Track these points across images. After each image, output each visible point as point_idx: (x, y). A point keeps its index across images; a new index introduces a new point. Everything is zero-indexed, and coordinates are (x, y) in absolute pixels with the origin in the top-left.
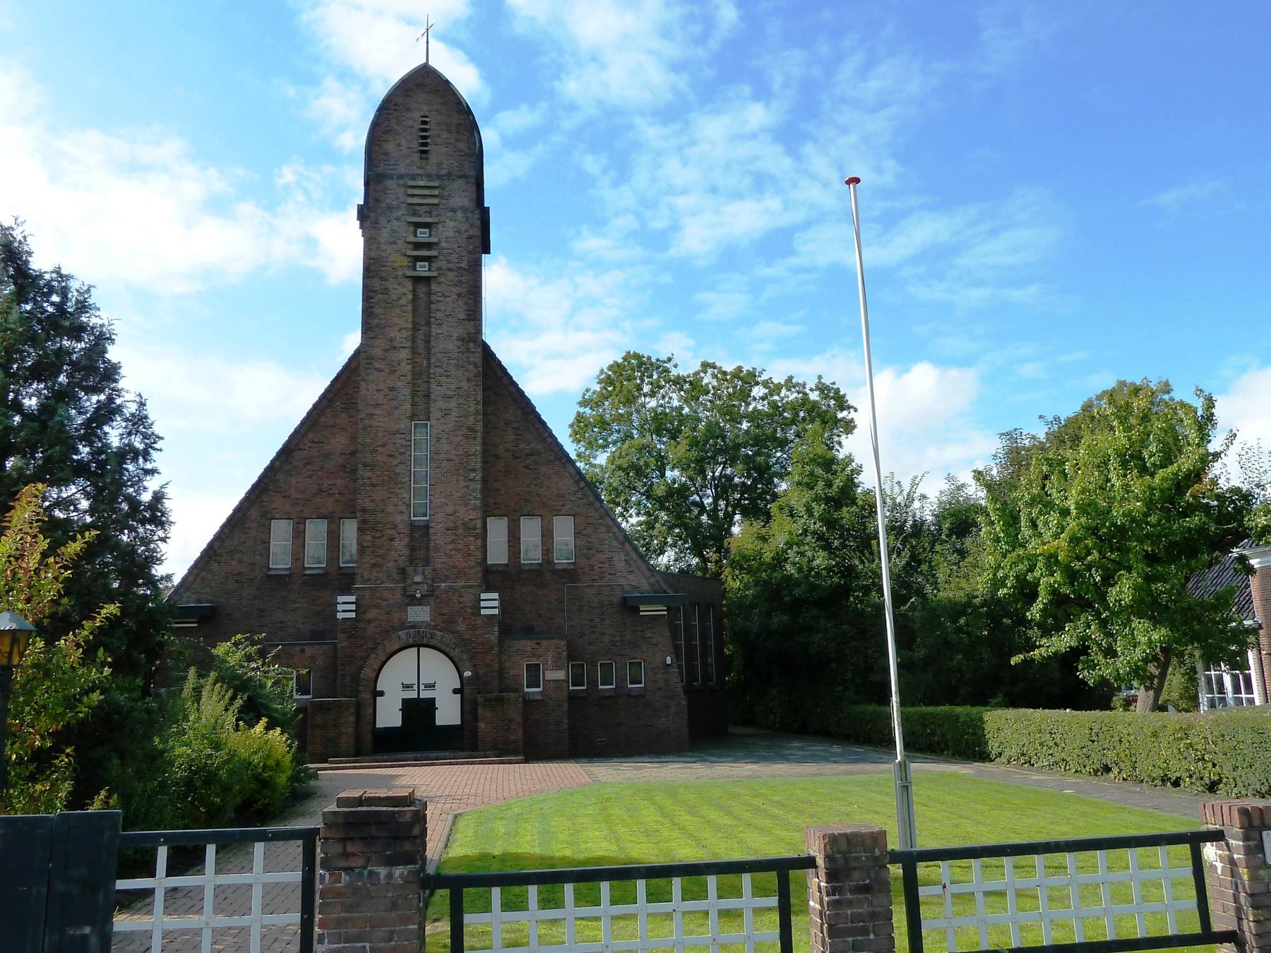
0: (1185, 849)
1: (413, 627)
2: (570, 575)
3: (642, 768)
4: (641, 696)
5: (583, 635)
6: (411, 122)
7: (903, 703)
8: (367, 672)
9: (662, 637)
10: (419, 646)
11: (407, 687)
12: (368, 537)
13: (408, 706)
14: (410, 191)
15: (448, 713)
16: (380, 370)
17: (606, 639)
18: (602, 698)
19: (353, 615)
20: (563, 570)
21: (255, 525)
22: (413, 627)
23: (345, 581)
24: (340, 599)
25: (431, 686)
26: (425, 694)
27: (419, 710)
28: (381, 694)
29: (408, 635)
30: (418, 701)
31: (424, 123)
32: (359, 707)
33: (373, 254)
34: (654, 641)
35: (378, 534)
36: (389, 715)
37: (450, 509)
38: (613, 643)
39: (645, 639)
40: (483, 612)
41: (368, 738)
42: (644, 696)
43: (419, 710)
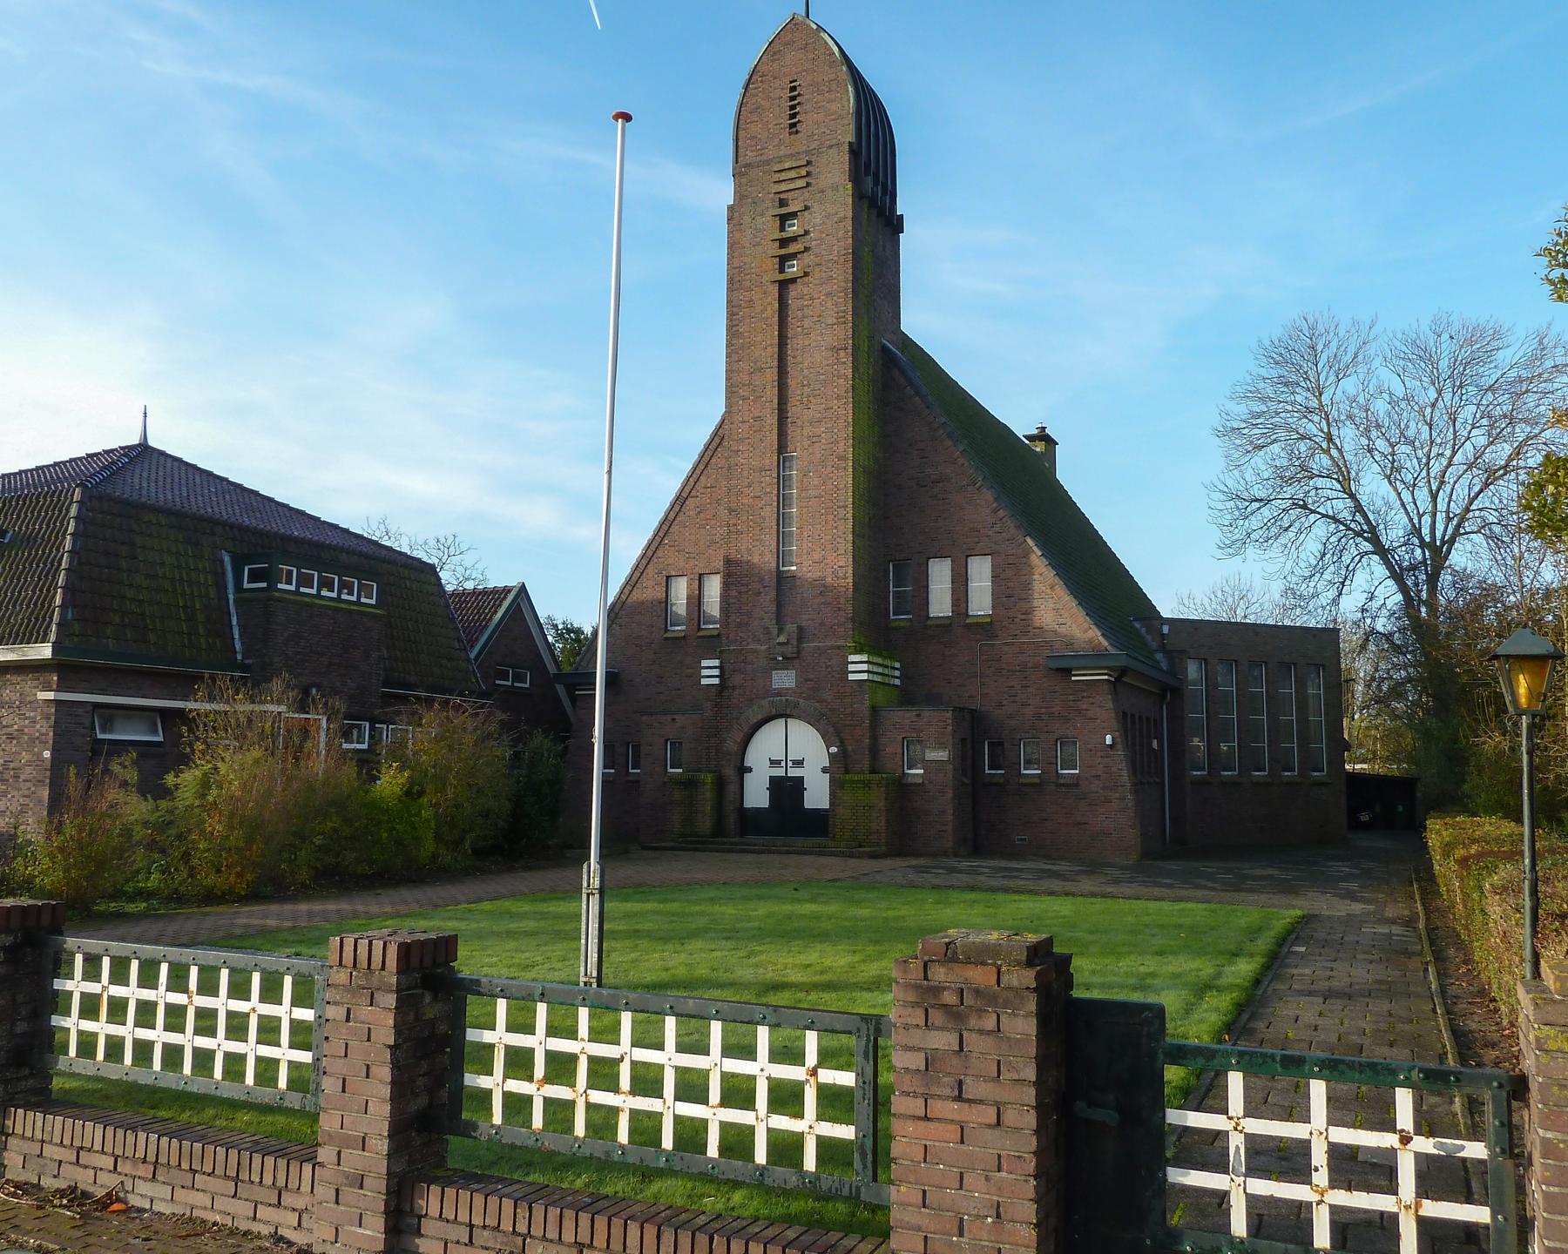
0: (92, 1172)
1: (779, 694)
2: (985, 628)
3: (207, 914)
4: (1075, 783)
5: (1000, 705)
6: (778, 93)
7: (602, 857)
8: (731, 745)
9: (1103, 709)
10: (787, 716)
11: (774, 763)
12: (734, 593)
13: (776, 785)
14: (777, 177)
15: (817, 795)
16: (744, 399)
17: (1028, 711)
18: (1024, 785)
19: (716, 681)
20: (977, 624)
21: (651, 583)
22: (779, 694)
23: (711, 644)
24: (705, 663)
25: (799, 763)
26: (794, 772)
27: (787, 789)
28: (750, 770)
29: (772, 704)
30: (786, 779)
31: (793, 89)
32: (720, 784)
33: (736, 263)
34: (1090, 714)
35: (744, 589)
36: (757, 795)
37: (816, 556)
38: (1039, 716)
39: (1079, 711)
40: (851, 677)
41: (732, 819)
42: (1077, 785)
43: (787, 789)
